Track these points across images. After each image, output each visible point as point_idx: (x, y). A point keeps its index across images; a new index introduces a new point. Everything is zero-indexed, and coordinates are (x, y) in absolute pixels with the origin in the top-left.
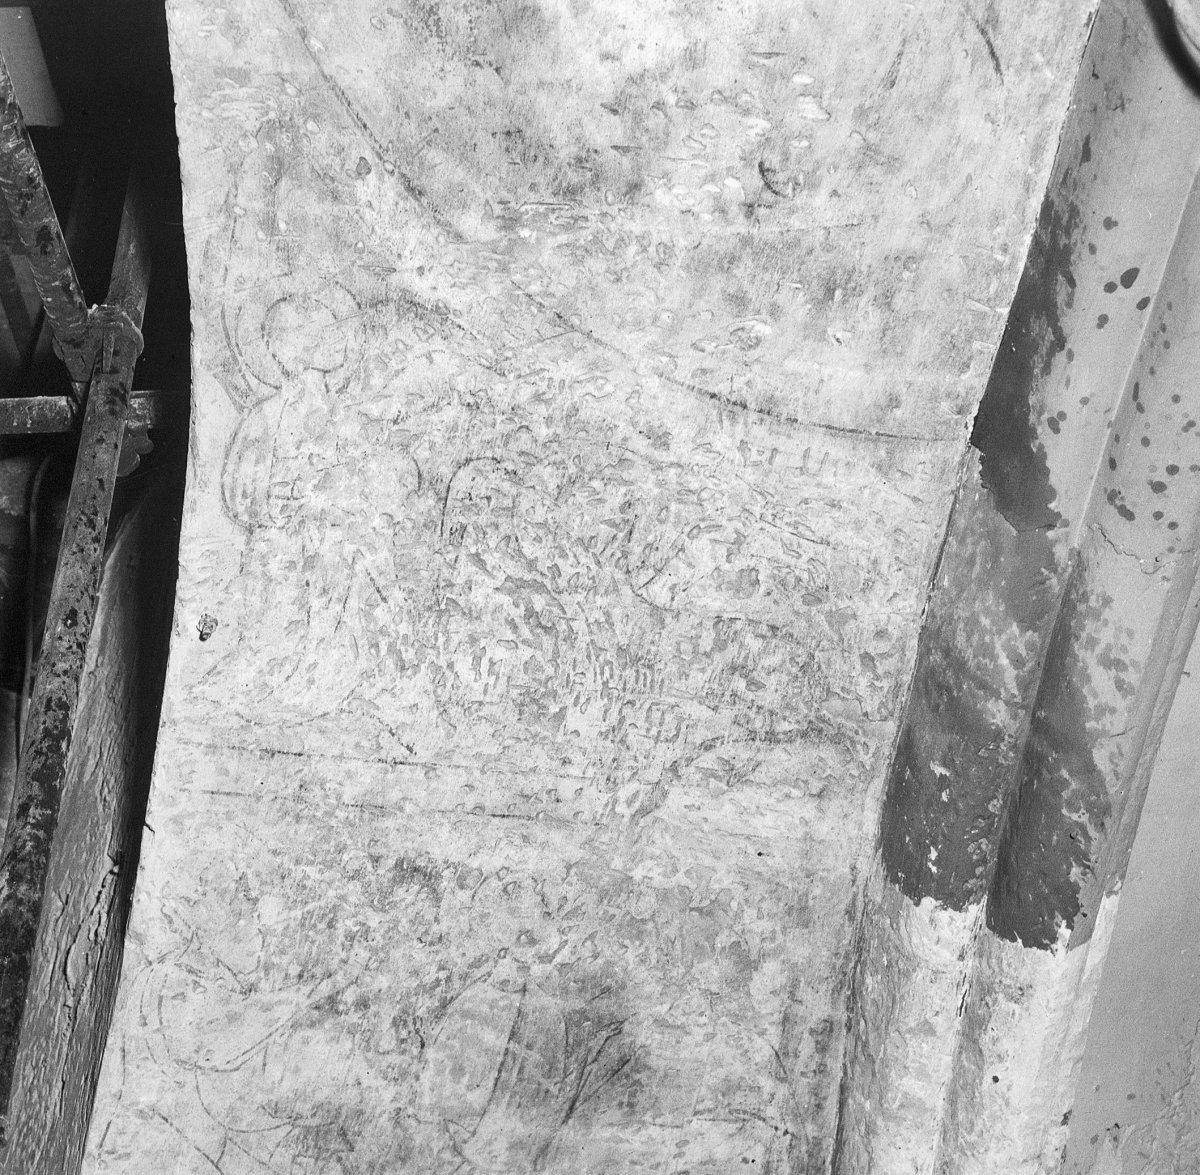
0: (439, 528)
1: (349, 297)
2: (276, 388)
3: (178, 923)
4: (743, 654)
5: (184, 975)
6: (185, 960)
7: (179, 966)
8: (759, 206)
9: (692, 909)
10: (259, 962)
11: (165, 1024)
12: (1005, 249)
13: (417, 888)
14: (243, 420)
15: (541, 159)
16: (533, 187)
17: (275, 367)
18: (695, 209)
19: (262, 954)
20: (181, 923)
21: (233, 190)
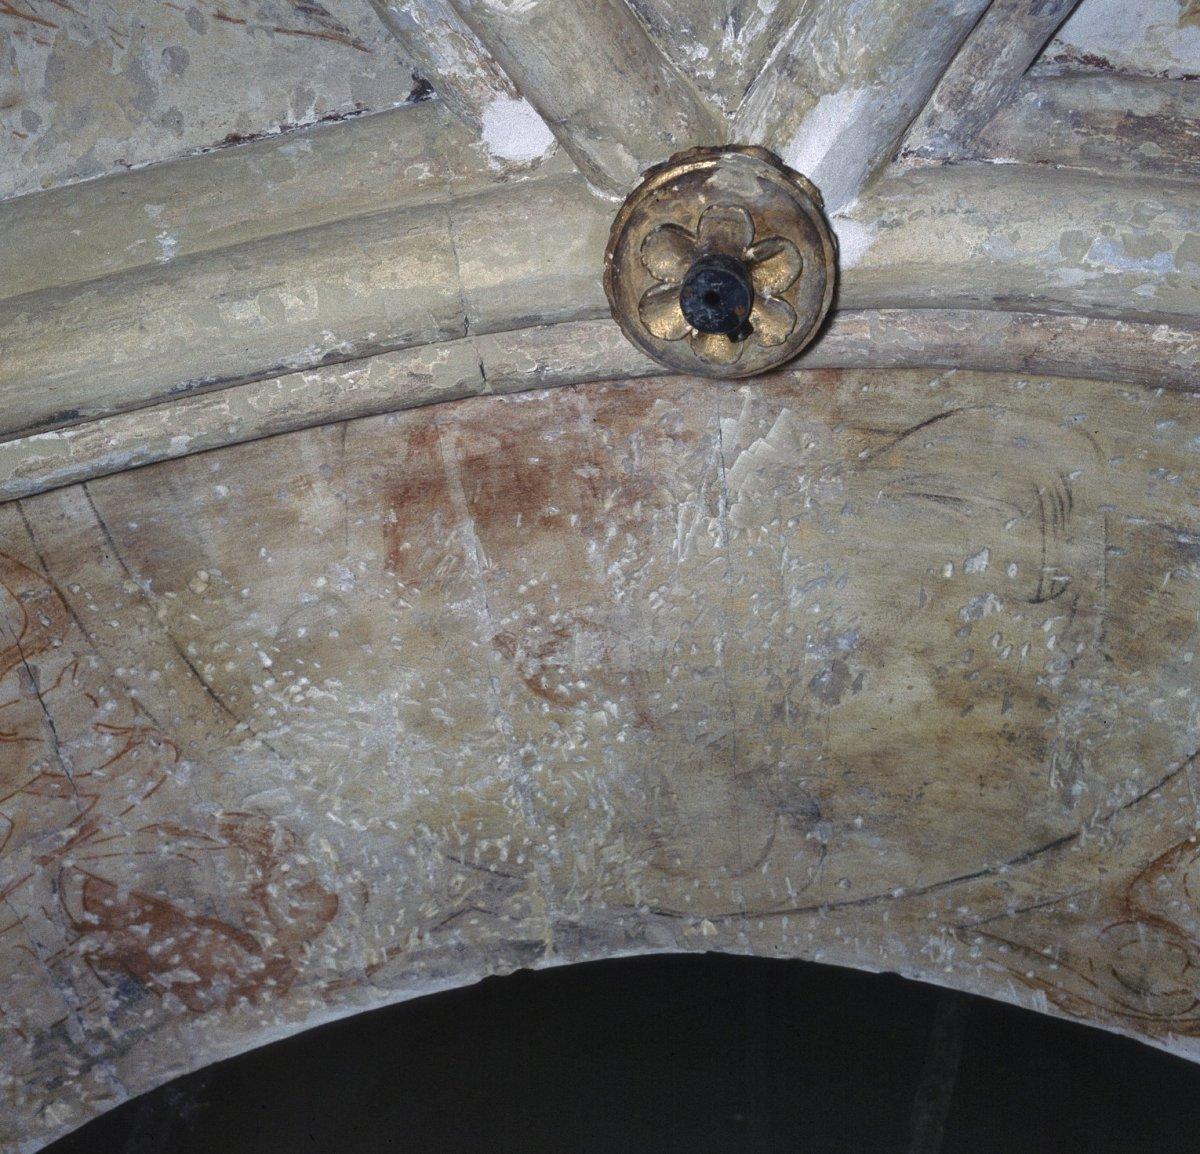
15: (1009, 766)
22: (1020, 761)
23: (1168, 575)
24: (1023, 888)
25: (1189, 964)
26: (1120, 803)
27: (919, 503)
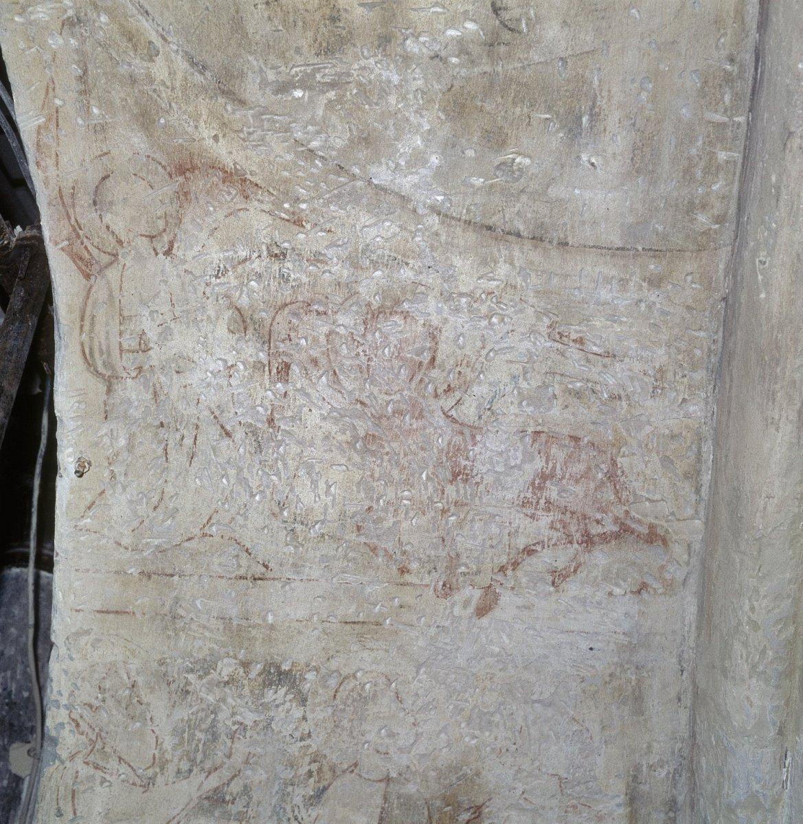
0: (267, 368)
1: (160, 168)
2: (114, 255)
3: (84, 727)
4: (551, 465)
5: (91, 771)
6: (91, 758)
7: (87, 763)
8: (499, 44)
9: (536, 701)
10: (154, 758)
11: (78, 814)
12: (732, 60)
13: (284, 690)
14: (91, 287)
16: (298, 50)
17: (110, 237)
18: (443, 54)
19: (156, 752)
20: (87, 726)
21: (51, 84)
22: (310, 34)
23: (548, 116)
24: (159, 70)
25: (152, 237)
26: (299, 135)
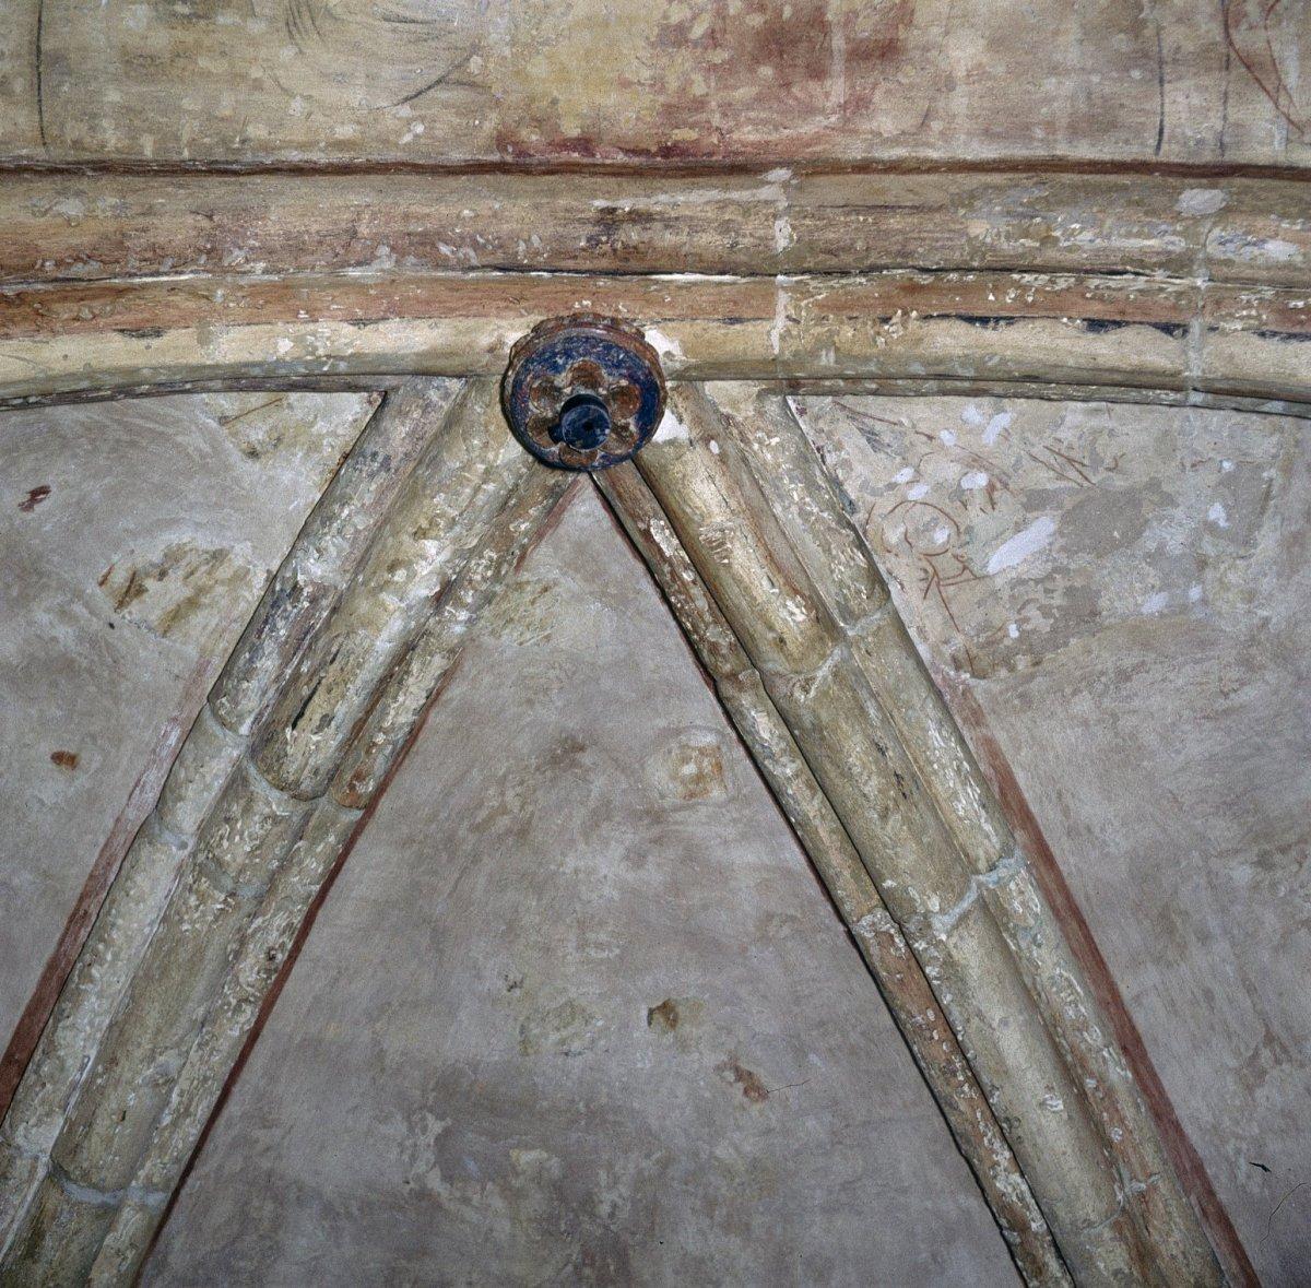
27: (420, 16)
